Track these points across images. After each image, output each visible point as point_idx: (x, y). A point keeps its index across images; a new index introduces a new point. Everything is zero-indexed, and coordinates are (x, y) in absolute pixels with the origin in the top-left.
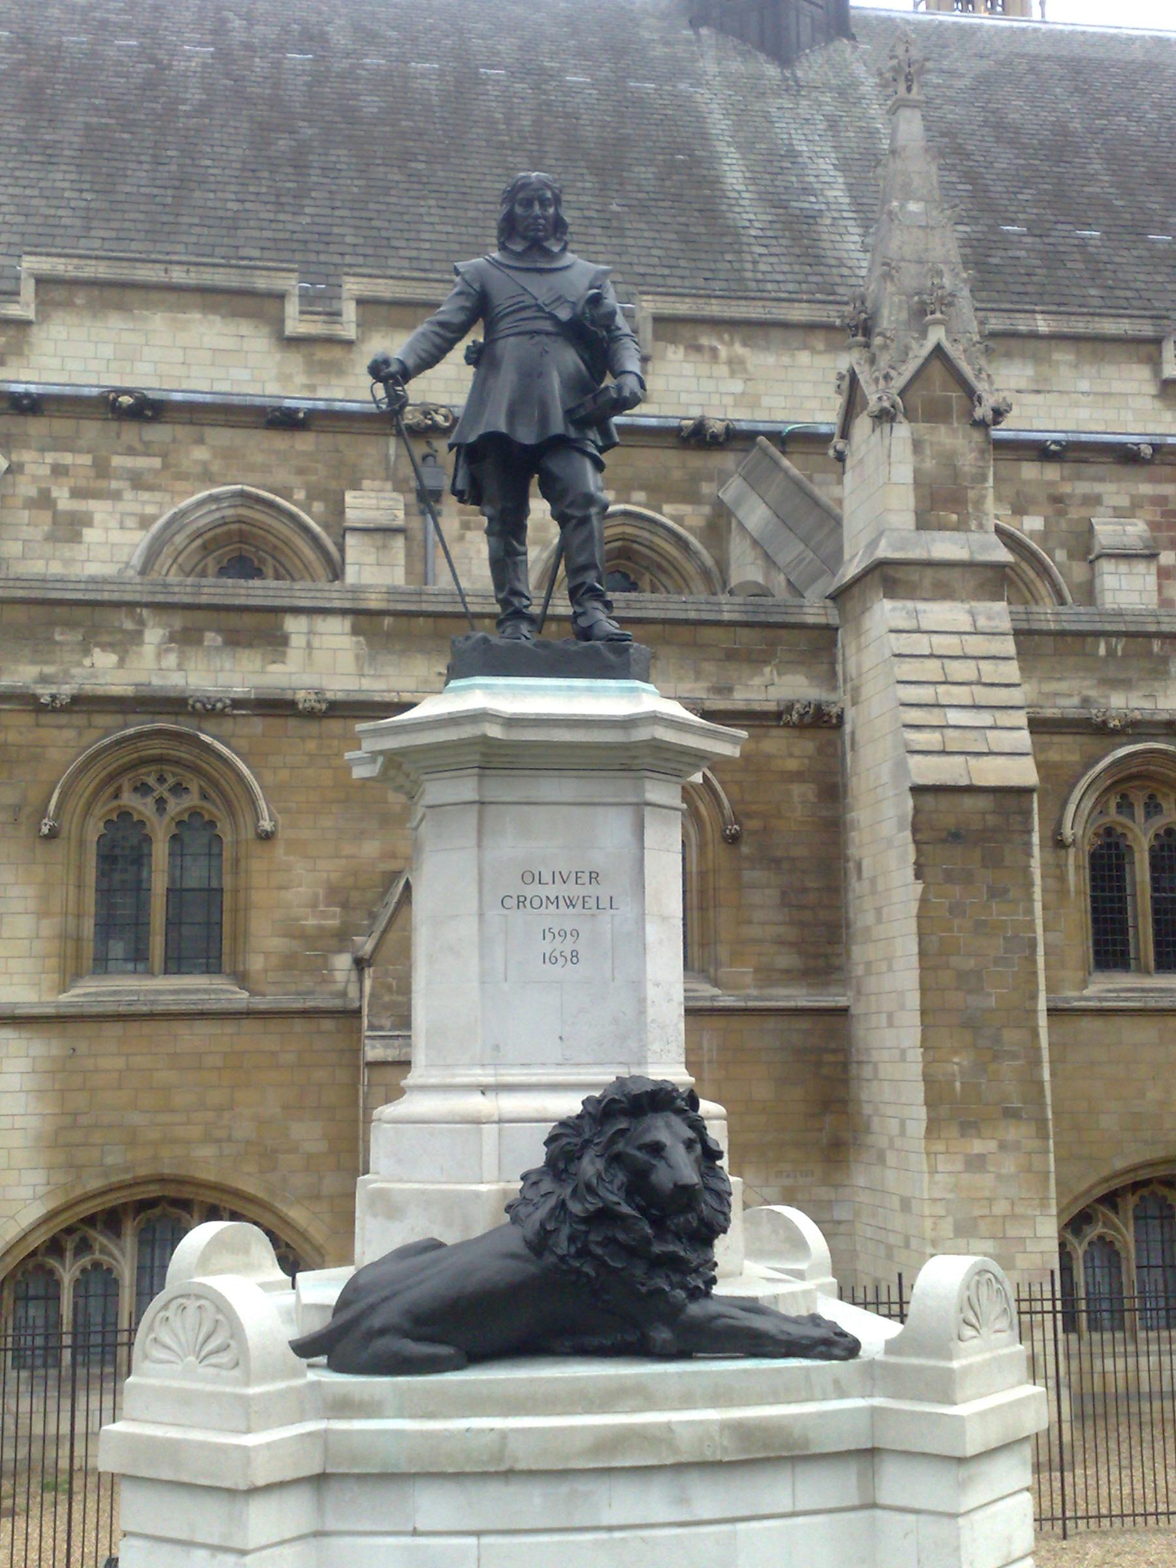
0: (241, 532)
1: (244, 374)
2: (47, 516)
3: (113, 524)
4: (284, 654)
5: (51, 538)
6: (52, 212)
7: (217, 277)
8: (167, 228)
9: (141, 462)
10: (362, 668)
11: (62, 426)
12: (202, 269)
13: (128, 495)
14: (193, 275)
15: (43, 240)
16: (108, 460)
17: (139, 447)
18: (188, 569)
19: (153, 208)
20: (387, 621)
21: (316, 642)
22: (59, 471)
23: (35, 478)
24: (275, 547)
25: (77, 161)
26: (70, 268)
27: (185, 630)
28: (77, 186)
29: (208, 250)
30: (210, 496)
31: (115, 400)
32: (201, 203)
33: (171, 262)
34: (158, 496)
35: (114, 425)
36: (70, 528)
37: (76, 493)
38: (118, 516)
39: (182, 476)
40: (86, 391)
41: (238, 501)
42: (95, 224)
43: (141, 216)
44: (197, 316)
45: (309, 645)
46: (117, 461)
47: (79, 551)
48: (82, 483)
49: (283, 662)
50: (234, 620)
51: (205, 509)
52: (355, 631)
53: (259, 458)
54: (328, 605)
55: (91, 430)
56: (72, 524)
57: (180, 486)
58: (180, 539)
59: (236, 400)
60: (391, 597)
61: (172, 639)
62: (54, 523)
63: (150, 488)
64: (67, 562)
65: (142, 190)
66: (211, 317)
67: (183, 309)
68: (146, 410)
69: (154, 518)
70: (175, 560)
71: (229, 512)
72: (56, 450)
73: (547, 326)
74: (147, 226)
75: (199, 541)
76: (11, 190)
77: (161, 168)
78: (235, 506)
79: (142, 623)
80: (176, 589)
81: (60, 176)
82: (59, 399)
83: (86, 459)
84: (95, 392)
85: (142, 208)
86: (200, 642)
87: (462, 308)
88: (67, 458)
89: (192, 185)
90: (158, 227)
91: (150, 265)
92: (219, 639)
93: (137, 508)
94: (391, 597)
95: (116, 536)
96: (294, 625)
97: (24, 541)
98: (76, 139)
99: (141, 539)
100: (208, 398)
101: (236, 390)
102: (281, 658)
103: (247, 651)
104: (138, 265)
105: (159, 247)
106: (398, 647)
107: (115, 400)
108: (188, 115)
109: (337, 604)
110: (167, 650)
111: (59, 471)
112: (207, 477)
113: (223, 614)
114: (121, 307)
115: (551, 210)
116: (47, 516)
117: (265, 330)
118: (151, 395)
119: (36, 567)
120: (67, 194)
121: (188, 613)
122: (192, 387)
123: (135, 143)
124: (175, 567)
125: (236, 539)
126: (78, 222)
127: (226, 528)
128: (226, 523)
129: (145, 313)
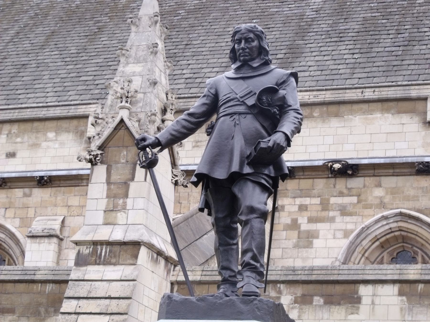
0: (403, 237)
1: (404, 145)
2: (295, 234)
3: (330, 236)
4: (358, 308)
5: (297, 246)
6: (336, 67)
7: (389, 93)
8: (395, 68)
9: (346, 200)
10: (404, 316)
11: (305, 183)
12: (381, 89)
13: (339, 219)
14: (376, 93)
15: (328, 83)
16: (328, 200)
17: (345, 191)
18: (373, 260)
19: (391, 58)
20: (421, 286)
21: (377, 301)
22: (302, 208)
23: (290, 212)
24: (422, 245)
25: (355, 38)
26: (311, 97)
27: (303, 295)
28: (351, 51)
29: (416, 77)
30: (383, 217)
31: (331, 166)
32: (418, 52)
33: (365, 88)
34: (355, 218)
35: (333, 180)
36: (307, 239)
37: (311, 220)
38: (332, 232)
39: (368, 206)
40: (316, 163)
41: (398, 218)
42: (357, 71)
43: (383, 63)
44: (379, 115)
45: (373, 303)
46: (333, 200)
47: (311, 252)
48: (314, 214)
49: (357, 313)
50: (330, 289)
51: (380, 224)
52: (401, 294)
53: (412, 192)
54: (384, 278)
55: (320, 184)
56: (308, 238)
57: (367, 212)
58: (365, 243)
59: (397, 161)
60: (423, 272)
61: (296, 302)
62: (299, 238)
63: (351, 214)
64: (304, 259)
65: (387, 49)
66: (386, 115)
67: (371, 112)
68: (348, 170)
69: (352, 231)
70: (363, 255)
71: (395, 225)
72: (301, 197)
73: (242, 109)
74: (384, 69)
75: (377, 243)
76: (317, 58)
77: (399, 36)
78: (397, 222)
79: (280, 292)
80: (299, 272)
81: (344, 47)
82: (303, 169)
83: (317, 201)
84: (321, 163)
85: (384, 59)
86: (311, 302)
87: (204, 104)
88: (307, 201)
89: (414, 43)
90: (390, 68)
91: (354, 91)
92: (322, 301)
93: (343, 226)
94: (423, 272)
95: (332, 243)
96: (364, 291)
97: (283, 248)
98: (357, 27)
99: (345, 243)
100: (382, 161)
101: (399, 155)
102: (356, 311)
103: (337, 307)
104: (348, 91)
105: (389, 79)
106: (426, 303)
107: (331, 166)
108: (421, 5)
109: (389, 277)
110: (293, 308)
111: (302, 208)
112: (382, 205)
113: (324, 286)
114: (337, 115)
115: (255, 43)
116: (295, 234)
117: (416, 119)
118: (350, 162)
119: (289, 263)
120: (345, 57)
121: (305, 286)
122: (375, 156)
123: (388, 24)
124: (363, 259)
125: (400, 241)
126: (348, 71)
127: (392, 234)
128: (392, 232)
129: (350, 117)
